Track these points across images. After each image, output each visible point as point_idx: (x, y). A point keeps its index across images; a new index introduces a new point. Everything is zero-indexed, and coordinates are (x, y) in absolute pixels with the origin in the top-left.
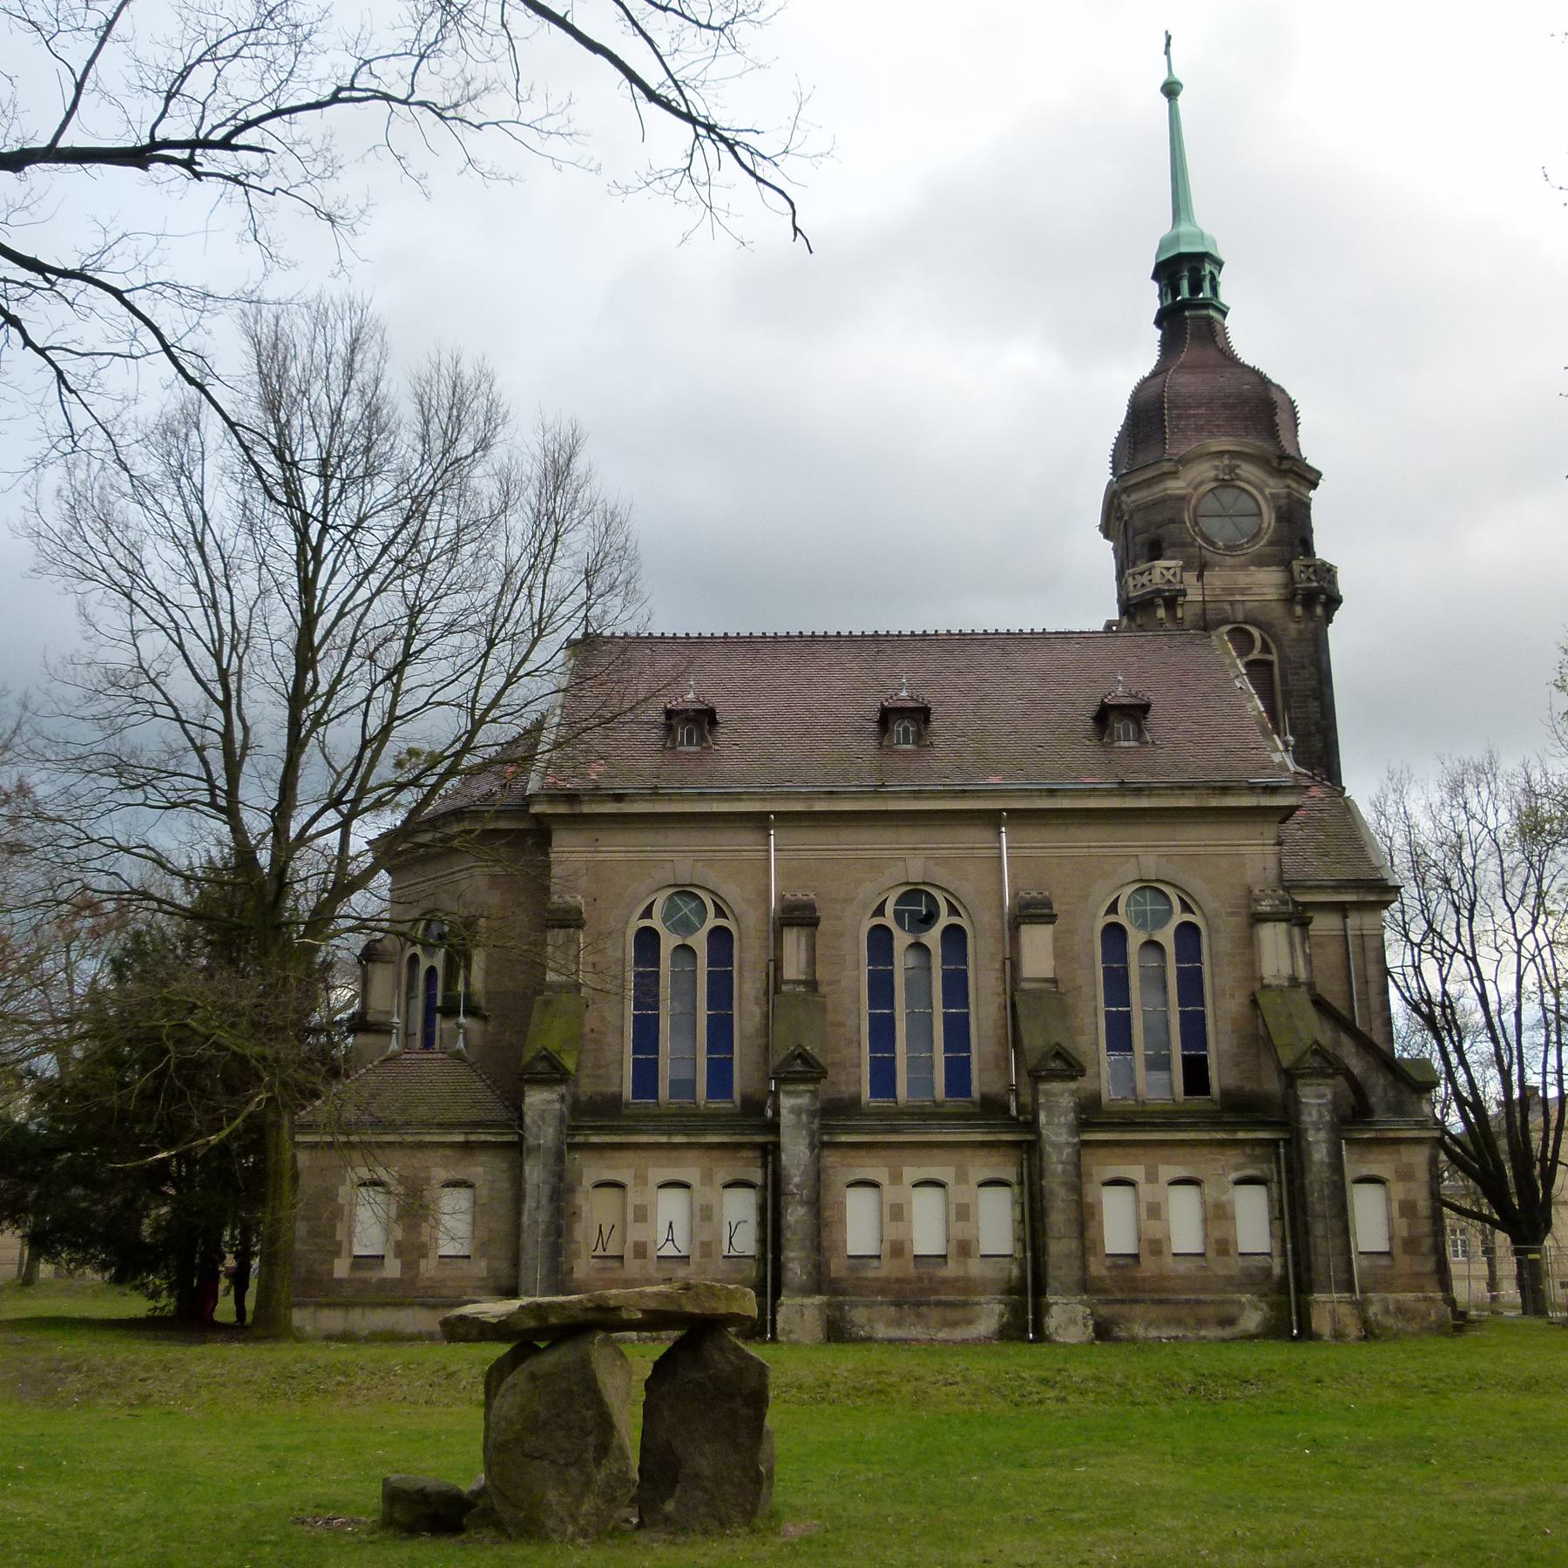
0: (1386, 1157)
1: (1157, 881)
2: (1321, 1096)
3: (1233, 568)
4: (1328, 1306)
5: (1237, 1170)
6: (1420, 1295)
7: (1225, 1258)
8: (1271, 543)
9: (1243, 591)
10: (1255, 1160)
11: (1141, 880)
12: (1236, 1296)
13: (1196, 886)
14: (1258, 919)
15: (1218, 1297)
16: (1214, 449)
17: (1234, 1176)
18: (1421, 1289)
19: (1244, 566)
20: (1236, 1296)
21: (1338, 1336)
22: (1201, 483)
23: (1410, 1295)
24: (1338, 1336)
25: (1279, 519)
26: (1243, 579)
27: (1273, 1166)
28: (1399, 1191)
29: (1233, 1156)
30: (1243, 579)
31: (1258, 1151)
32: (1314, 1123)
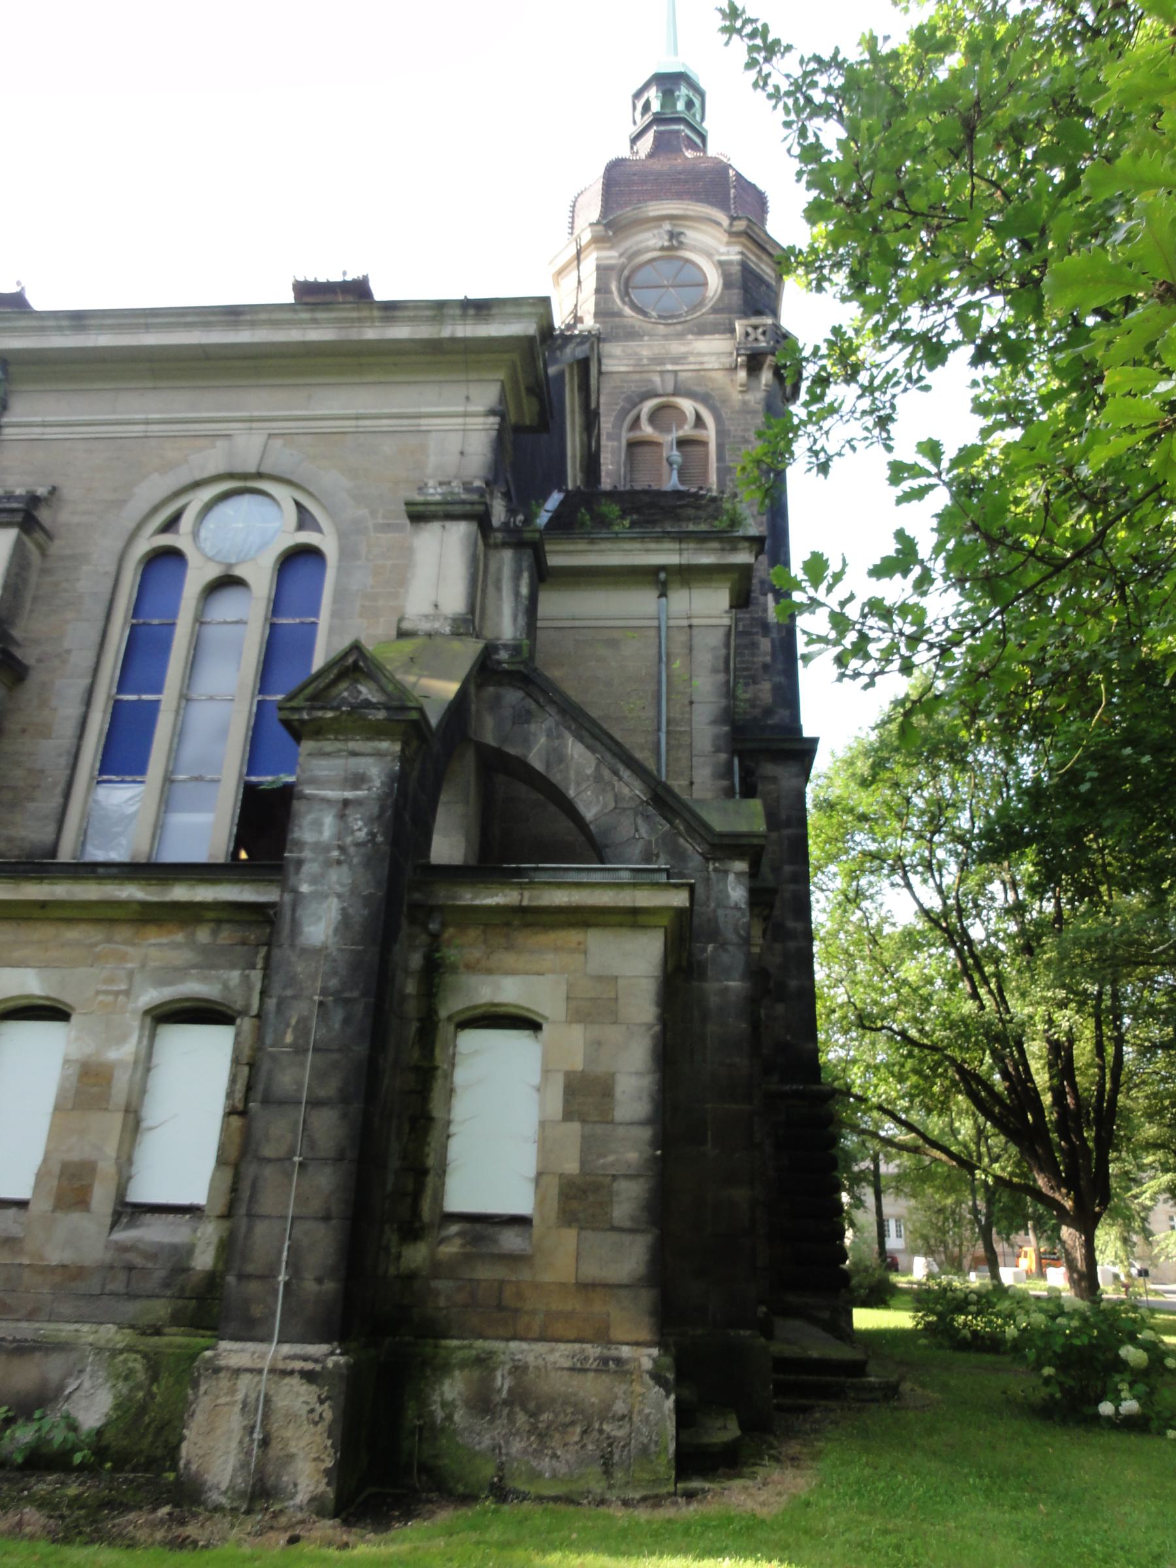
0: (549, 960)
1: (259, 476)
2: (357, 781)
3: (666, 337)
4: (245, 1380)
5: (160, 983)
6: (593, 1351)
7: (76, 1218)
8: (715, 310)
9: (677, 360)
10: (209, 960)
11: (231, 476)
12: (66, 1330)
13: (331, 479)
14: (419, 515)
15: (26, 1329)
16: (652, 214)
17: (151, 996)
18: (602, 1336)
19: (680, 336)
20: (66, 1330)
21: (260, 1492)
22: (637, 253)
23: (560, 1354)
24: (260, 1492)
25: (727, 285)
26: (676, 348)
27: (256, 976)
28: (570, 1043)
29: (161, 947)
30: (676, 348)
31: (227, 935)
32: (323, 848)
